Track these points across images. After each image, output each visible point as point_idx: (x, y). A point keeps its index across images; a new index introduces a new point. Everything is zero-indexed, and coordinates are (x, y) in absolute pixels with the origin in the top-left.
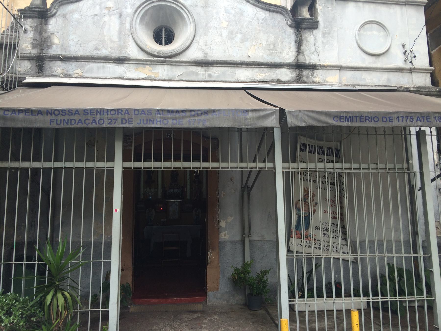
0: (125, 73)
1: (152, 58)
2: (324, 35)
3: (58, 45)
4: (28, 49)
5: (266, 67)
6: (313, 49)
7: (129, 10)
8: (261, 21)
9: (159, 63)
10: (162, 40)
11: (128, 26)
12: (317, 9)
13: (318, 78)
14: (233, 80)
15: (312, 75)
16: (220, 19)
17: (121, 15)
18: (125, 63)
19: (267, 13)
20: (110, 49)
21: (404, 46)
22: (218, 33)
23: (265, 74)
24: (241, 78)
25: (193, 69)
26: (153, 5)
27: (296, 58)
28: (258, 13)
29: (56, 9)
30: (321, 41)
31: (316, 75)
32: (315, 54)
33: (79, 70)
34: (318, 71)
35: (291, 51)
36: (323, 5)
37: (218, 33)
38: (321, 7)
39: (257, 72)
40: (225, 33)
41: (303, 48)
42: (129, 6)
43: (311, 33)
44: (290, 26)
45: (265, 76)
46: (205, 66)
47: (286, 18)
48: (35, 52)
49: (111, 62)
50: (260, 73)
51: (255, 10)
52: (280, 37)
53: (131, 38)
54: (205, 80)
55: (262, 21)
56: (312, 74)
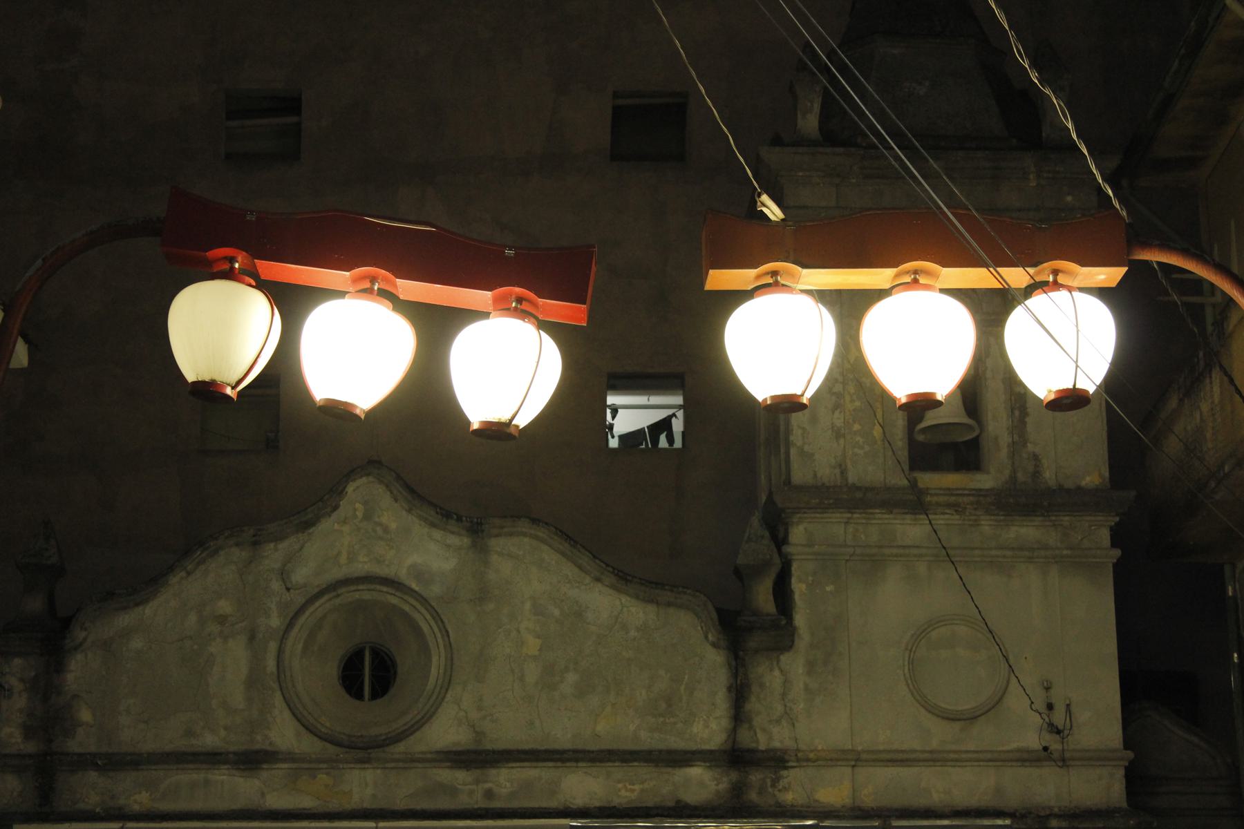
0: (263, 795)
1: (332, 749)
2: (811, 667)
3: (91, 727)
4: (13, 740)
5: (646, 764)
6: (780, 709)
7: (275, 622)
8: (633, 633)
9: (352, 766)
10: (362, 683)
11: (271, 665)
12: (792, 592)
13: (791, 793)
14: (553, 804)
15: (773, 786)
16: (519, 631)
17: (252, 638)
18: (263, 769)
19: (651, 609)
20: (223, 733)
21: (1047, 689)
22: (513, 671)
23: (641, 786)
24: (574, 799)
25: (445, 775)
26: (338, 601)
27: (729, 736)
28: (625, 609)
29: (86, 629)
30: (801, 685)
31: (787, 786)
32: (784, 723)
33: (144, 793)
34: (792, 772)
35: (716, 718)
36: (810, 578)
37: (513, 671)
38: (803, 586)
39: (619, 781)
40: (532, 673)
41: (753, 705)
42: (273, 606)
43: (775, 663)
44: (714, 645)
45: (642, 791)
46: (476, 768)
47: (703, 624)
48: (31, 747)
49: (226, 767)
50: (627, 785)
51: (618, 602)
52: (686, 677)
53: (278, 700)
54: (476, 807)
55: (636, 634)
56: (775, 782)
